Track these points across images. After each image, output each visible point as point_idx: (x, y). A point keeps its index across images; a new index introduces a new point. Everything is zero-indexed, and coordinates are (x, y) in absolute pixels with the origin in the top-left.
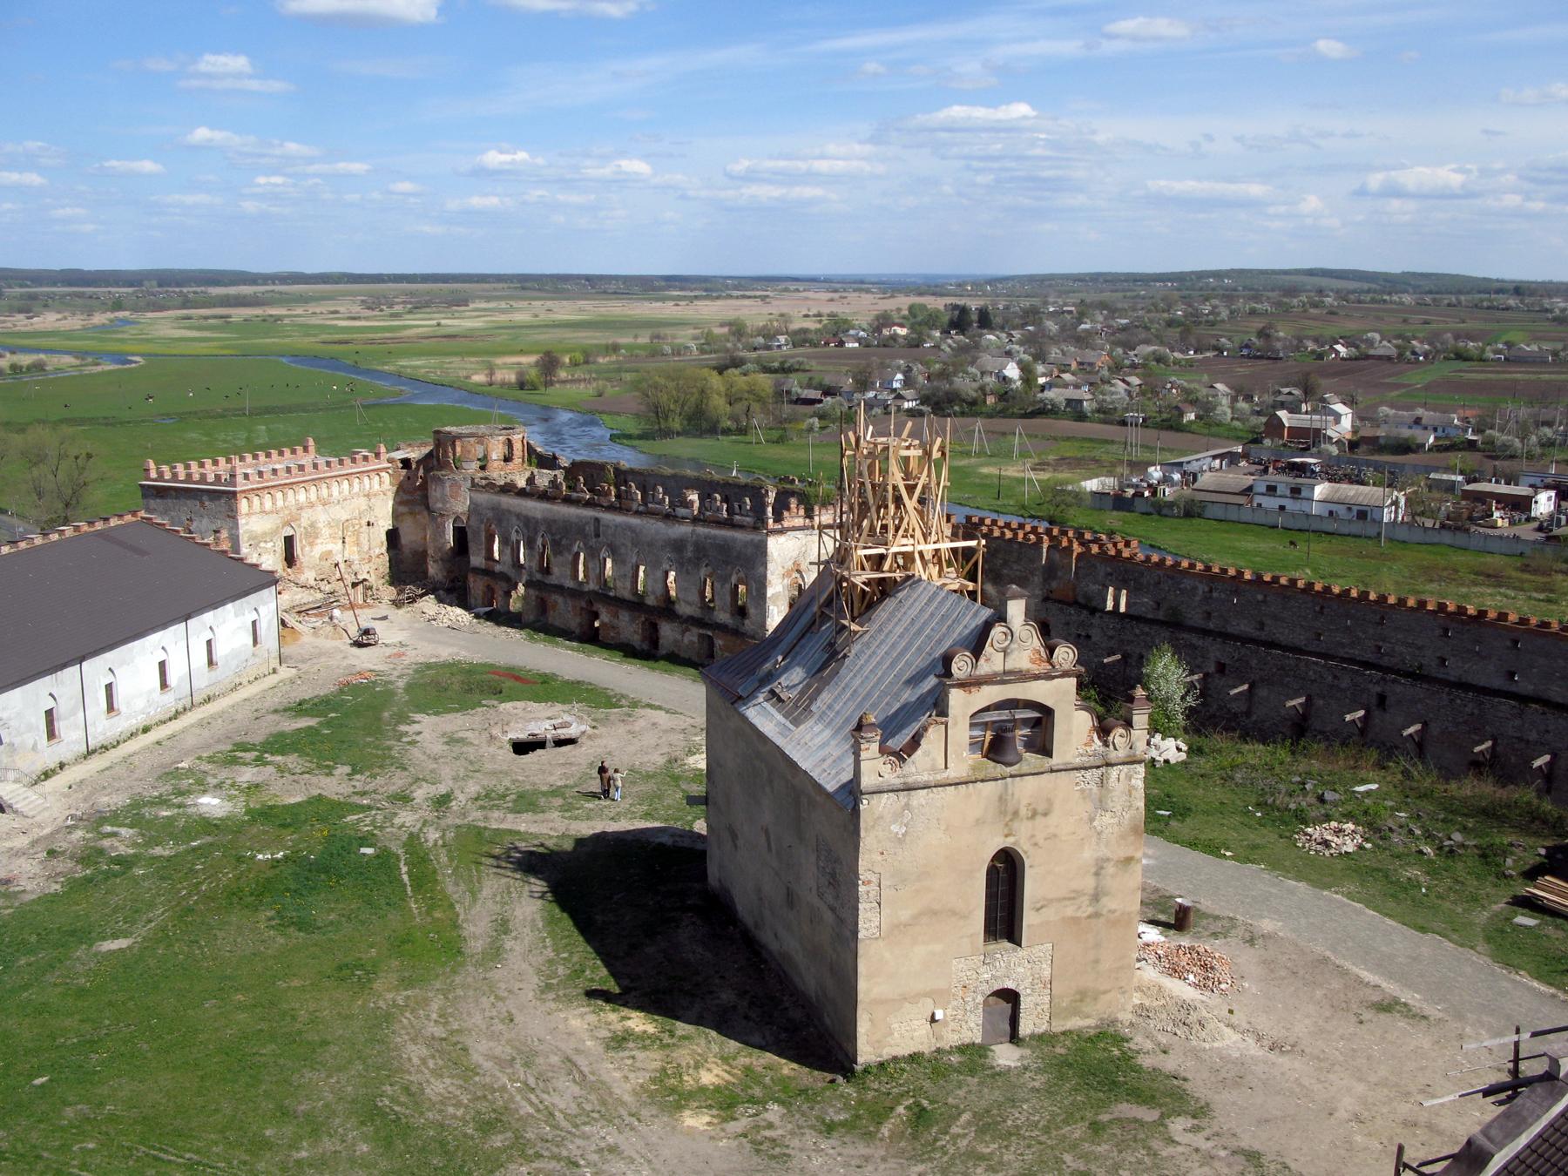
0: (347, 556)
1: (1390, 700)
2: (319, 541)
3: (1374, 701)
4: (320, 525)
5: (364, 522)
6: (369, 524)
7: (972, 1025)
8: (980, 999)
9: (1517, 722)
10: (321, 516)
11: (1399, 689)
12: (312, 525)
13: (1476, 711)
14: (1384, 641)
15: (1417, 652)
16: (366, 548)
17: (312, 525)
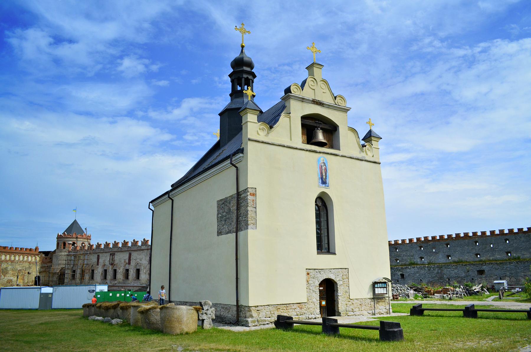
0: (18, 282)
1: (406, 275)
2: (8, 275)
3: (400, 277)
4: (9, 269)
5: (27, 272)
6: (28, 273)
7: (314, 300)
8: (317, 283)
9: (456, 271)
10: (10, 267)
11: (408, 270)
12: (6, 268)
13: (439, 271)
14: (399, 257)
15: (412, 258)
16: (26, 282)
17: (6, 268)
